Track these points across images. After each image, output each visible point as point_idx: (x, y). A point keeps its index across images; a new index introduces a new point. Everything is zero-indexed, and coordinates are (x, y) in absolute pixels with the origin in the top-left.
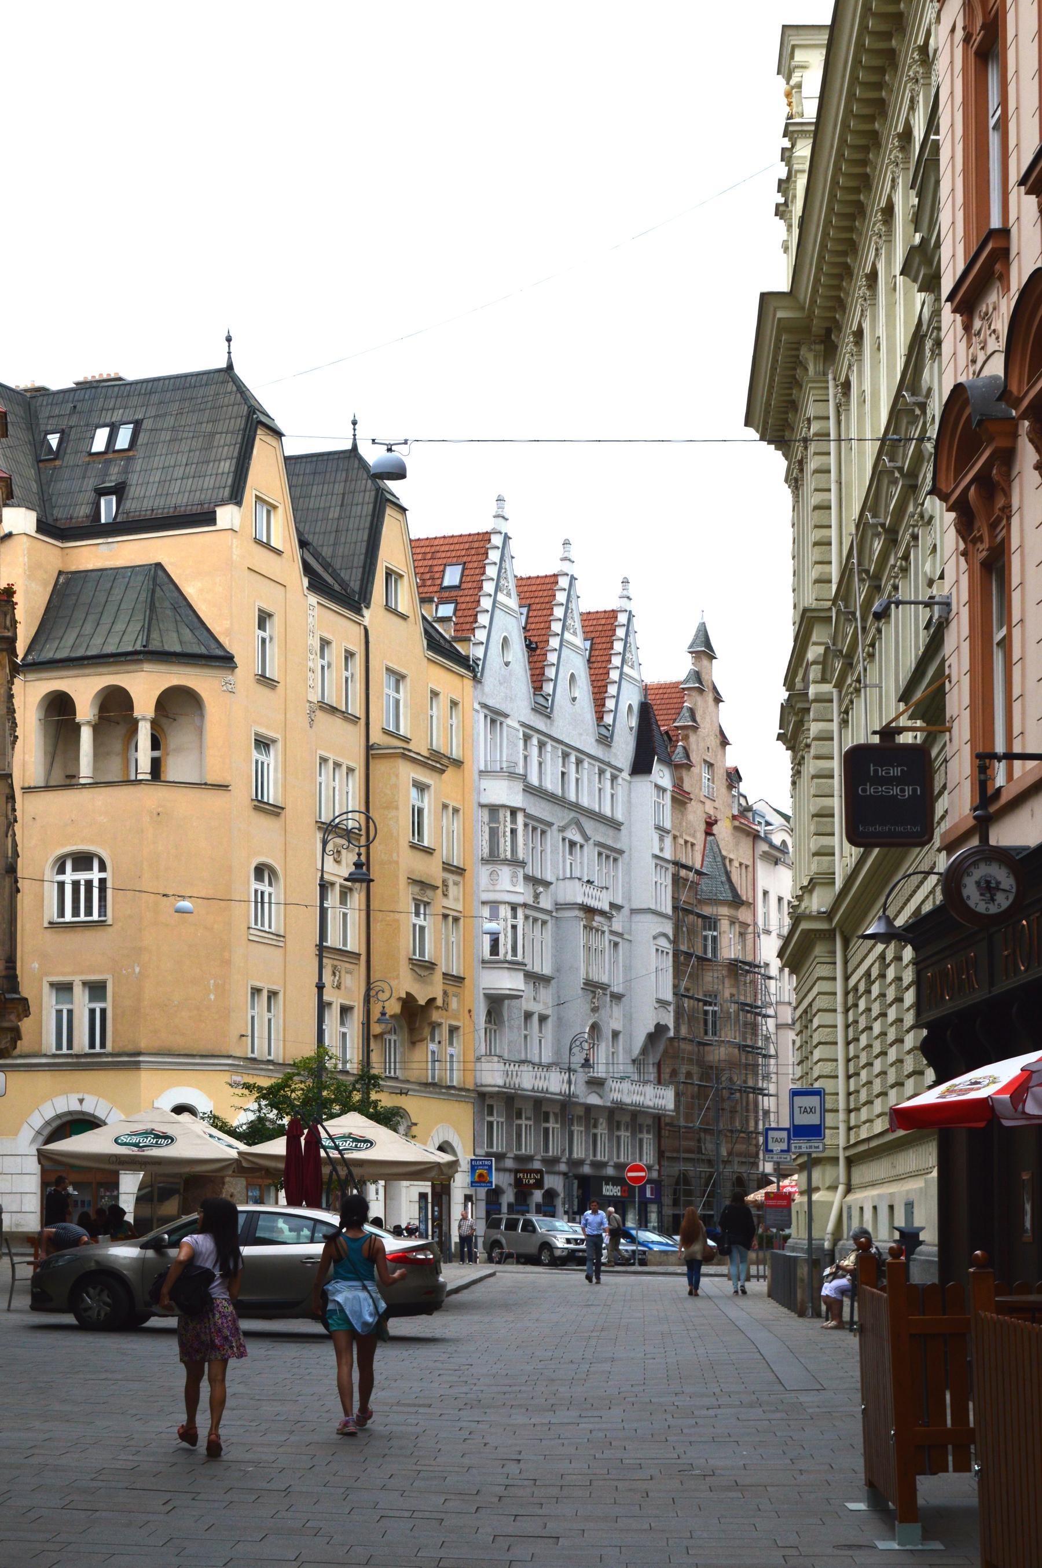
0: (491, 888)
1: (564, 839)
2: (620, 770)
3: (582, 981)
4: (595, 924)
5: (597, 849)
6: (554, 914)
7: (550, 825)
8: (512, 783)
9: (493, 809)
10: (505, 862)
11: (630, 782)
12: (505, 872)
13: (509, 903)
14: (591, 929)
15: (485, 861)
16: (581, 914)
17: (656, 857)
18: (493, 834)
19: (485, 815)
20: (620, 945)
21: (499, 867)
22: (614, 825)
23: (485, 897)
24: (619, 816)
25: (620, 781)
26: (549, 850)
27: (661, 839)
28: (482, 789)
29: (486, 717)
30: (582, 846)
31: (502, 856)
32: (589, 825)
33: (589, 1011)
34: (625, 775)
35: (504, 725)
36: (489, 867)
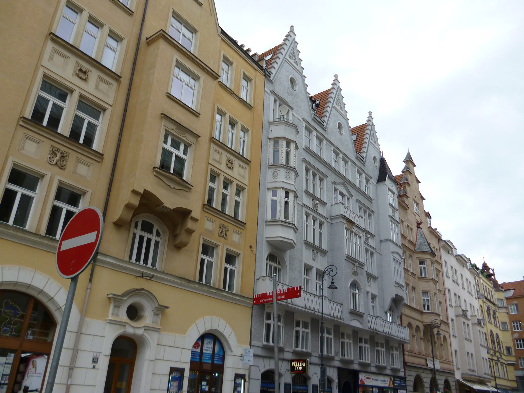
0: (274, 180)
1: (336, 190)
2: (371, 178)
3: (345, 255)
4: (353, 230)
5: (358, 204)
6: (329, 220)
7: (326, 177)
8: (287, 128)
9: (276, 141)
10: (282, 166)
11: (377, 186)
12: (282, 173)
13: (283, 188)
14: (352, 232)
15: (270, 167)
16: (345, 222)
17: (390, 216)
18: (276, 152)
19: (271, 143)
20: (375, 254)
21: (278, 169)
22: (370, 200)
23: (270, 186)
24: (371, 195)
25: (371, 182)
26: (325, 189)
27: (393, 212)
28: (270, 131)
29: (275, 101)
30: (348, 199)
31: (280, 163)
32: (353, 192)
33: (351, 274)
34: (374, 181)
35: (291, 113)
36: (272, 170)
